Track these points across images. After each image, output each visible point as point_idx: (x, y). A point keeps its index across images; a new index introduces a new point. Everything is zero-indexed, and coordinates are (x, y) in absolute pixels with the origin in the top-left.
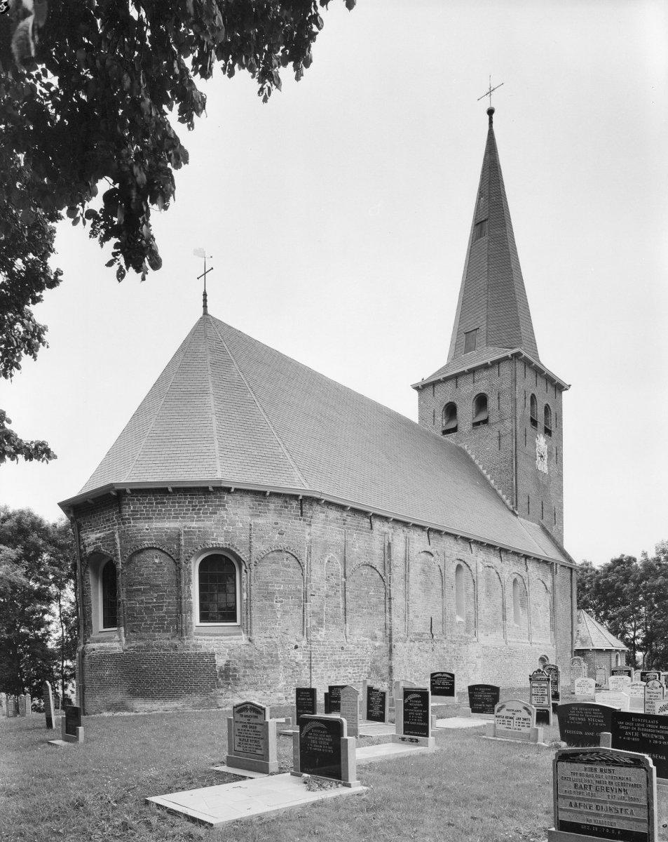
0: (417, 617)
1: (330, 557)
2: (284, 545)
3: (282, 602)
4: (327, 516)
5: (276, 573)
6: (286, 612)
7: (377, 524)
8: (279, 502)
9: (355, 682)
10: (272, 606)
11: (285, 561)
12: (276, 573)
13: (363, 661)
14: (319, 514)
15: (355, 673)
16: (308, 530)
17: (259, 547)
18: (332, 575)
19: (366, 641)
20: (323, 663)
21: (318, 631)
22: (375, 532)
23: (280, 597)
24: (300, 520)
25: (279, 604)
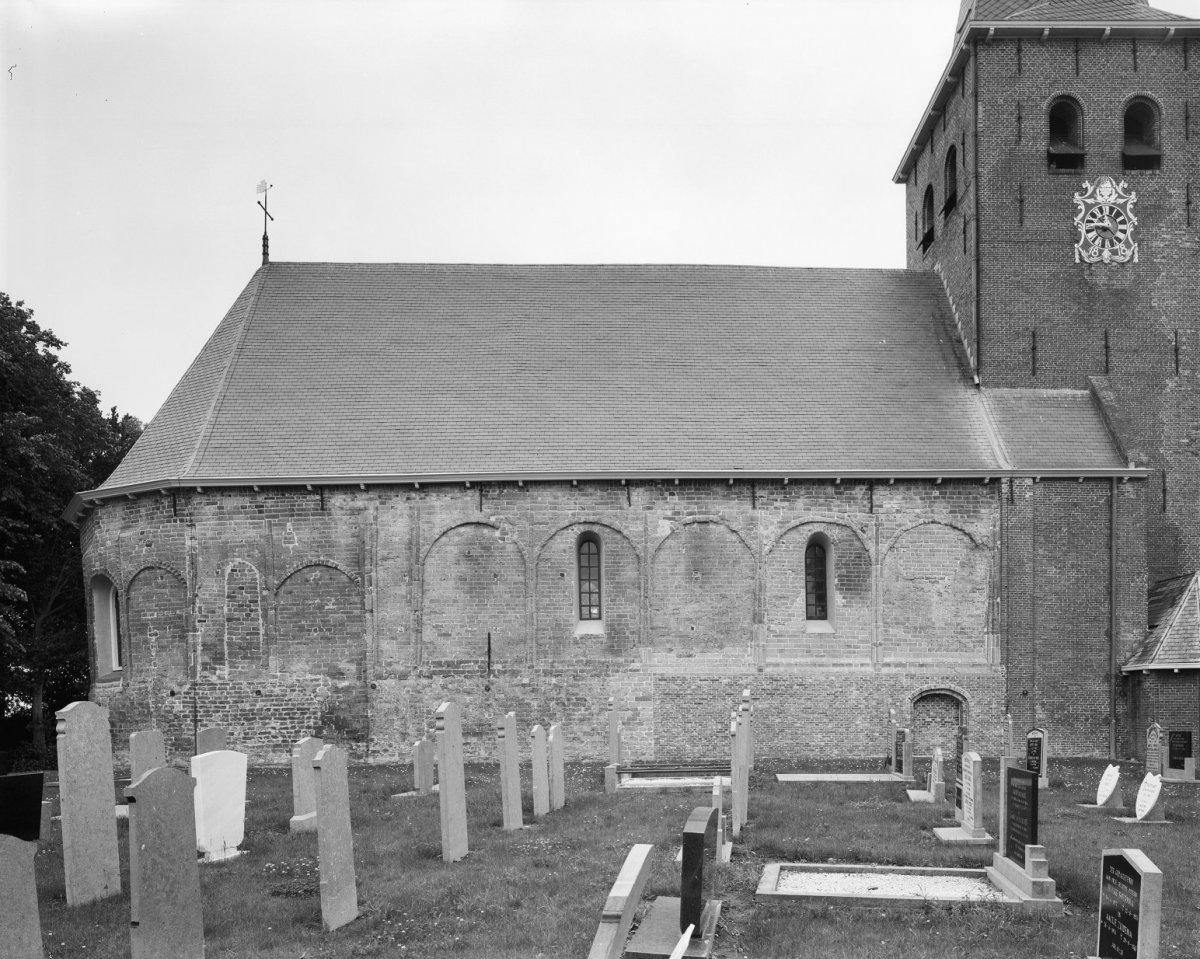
0: (447, 635)
1: (237, 564)
2: (153, 559)
3: (156, 635)
4: (221, 508)
5: (148, 597)
6: (162, 648)
7: (337, 500)
8: (119, 511)
9: (283, 741)
10: (146, 641)
11: (159, 581)
12: (148, 597)
13: (303, 711)
14: (206, 512)
15: (287, 728)
16: (188, 532)
17: (128, 568)
18: (242, 588)
19: (318, 680)
20: (221, 714)
21: (215, 669)
22: (337, 514)
23: (154, 628)
24: (175, 521)
25: (154, 638)
